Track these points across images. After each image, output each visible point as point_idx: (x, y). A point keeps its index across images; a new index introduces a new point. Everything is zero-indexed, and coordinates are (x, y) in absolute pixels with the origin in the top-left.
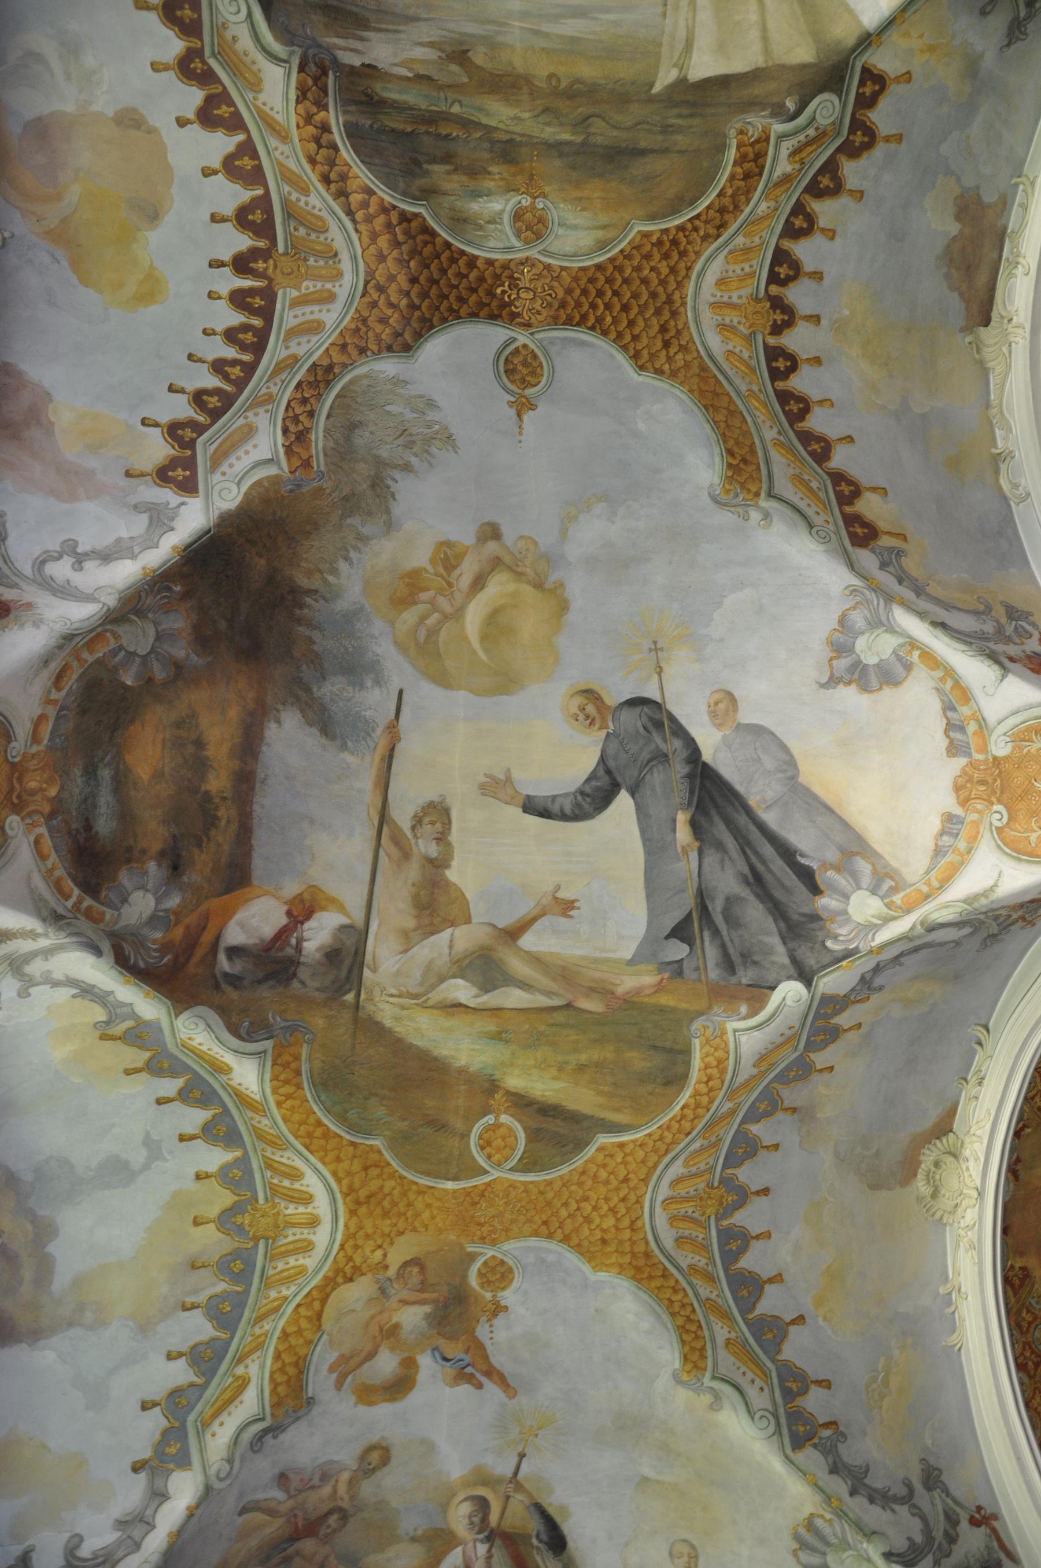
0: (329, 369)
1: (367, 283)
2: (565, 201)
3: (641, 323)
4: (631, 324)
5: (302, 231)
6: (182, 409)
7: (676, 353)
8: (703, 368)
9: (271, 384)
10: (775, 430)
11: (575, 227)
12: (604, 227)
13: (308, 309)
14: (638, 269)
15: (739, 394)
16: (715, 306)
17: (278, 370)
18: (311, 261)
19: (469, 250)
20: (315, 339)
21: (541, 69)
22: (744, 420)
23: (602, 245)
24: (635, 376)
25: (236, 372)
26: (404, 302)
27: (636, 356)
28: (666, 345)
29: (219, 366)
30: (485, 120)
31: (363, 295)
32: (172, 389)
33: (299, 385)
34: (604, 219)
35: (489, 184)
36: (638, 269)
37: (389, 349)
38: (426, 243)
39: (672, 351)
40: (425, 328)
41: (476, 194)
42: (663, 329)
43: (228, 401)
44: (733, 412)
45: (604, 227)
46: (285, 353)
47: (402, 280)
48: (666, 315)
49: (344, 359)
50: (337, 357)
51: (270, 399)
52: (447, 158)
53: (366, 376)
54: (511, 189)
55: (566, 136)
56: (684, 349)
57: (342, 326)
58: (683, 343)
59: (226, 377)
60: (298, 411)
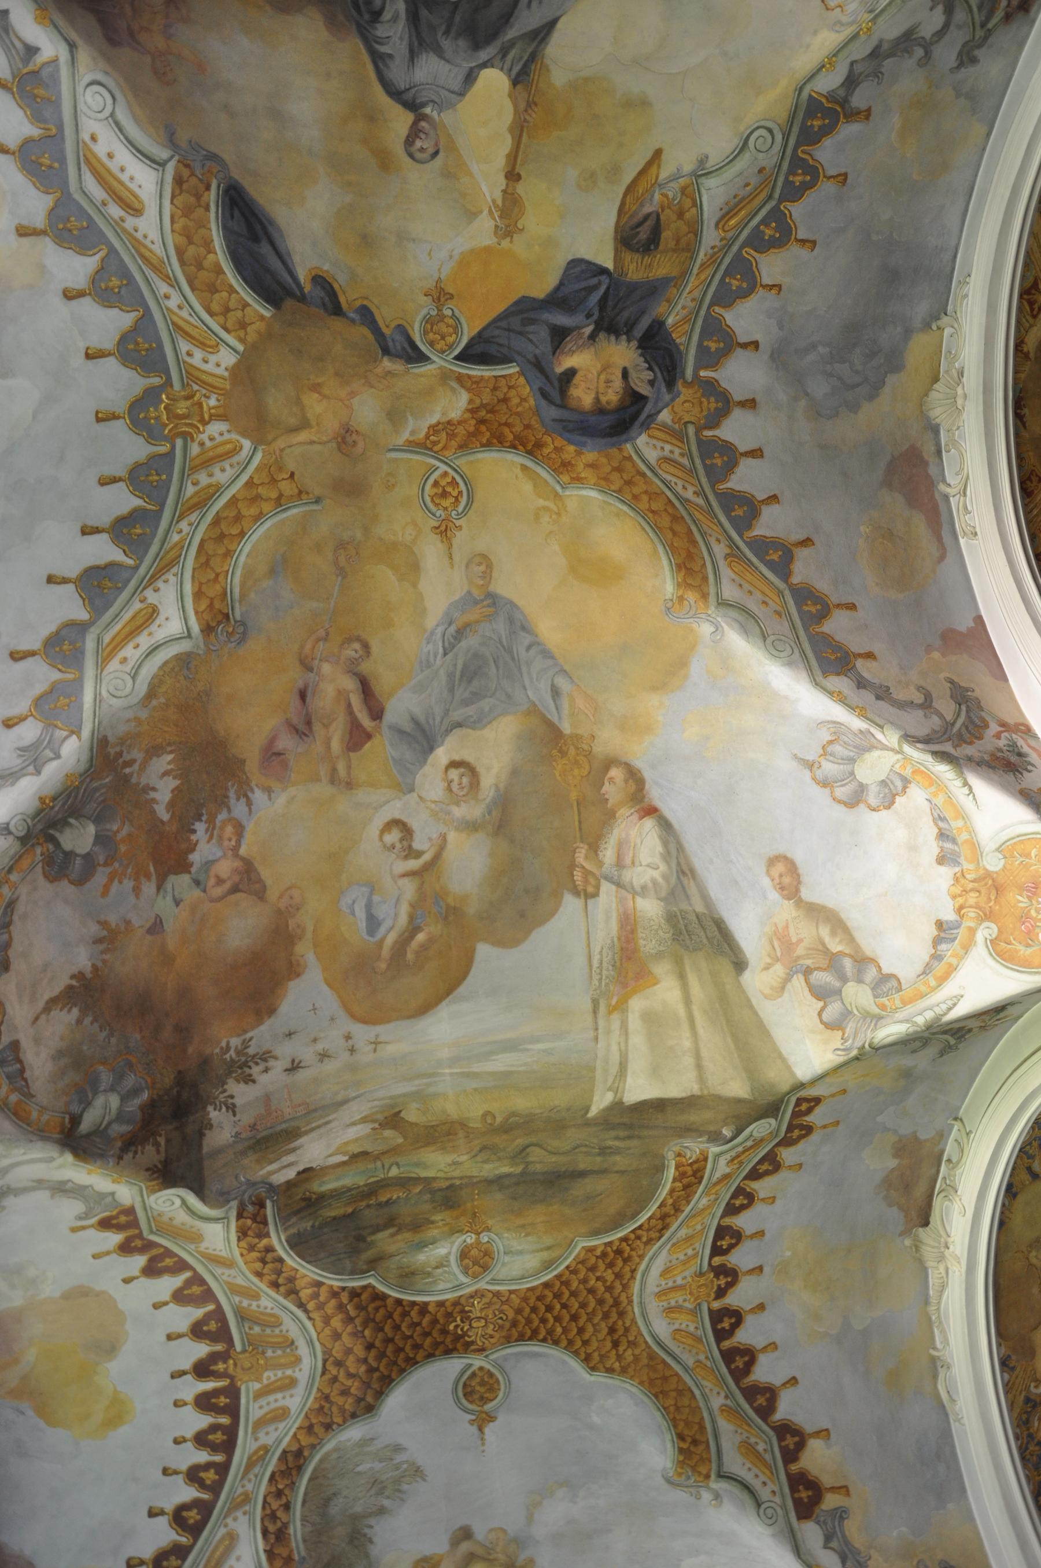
0: (299, 1453)
1: (325, 1361)
2: (508, 1230)
3: (590, 1329)
4: (581, 1331)
5: (257, 1329)
7: (625, 1350)
8: (652, 1356)
9: (245, 1482)
10: (723, 1394)
11: (520, 1253)
12: (549, 1248)
14: (584, 1281)
15: (686, 1369)
16: (661, 1294)
17: (250, 1465)
18: (269, 1353)
20: (281, 1426)
21: (474, 1110)
22: (693, 1396)
23: (548, 1265)
26: (363, 1369)
28: (616, 1344)
29: (193, 1475)
30: (424, 1174)
31: (323, 1373)
35: (434, 1232)
36: (584, 1281)
37: (354, 1416)
38: (377, 1309)
39: (621, 1349)
41: (422, 1246)
42: (612, 1330)
44: (683, 1391)
45: (549, 1248)
47: (359, 1350)
48: (614, 1316)
49: (312, 1440)
50: (305, 1441)
51: (247, 1498)
52: (390, 1222)
53: (336, 1449)
55: (505, 1170)
56: (632, 1344)
57: (306, 1409)
58: (631, 1338)
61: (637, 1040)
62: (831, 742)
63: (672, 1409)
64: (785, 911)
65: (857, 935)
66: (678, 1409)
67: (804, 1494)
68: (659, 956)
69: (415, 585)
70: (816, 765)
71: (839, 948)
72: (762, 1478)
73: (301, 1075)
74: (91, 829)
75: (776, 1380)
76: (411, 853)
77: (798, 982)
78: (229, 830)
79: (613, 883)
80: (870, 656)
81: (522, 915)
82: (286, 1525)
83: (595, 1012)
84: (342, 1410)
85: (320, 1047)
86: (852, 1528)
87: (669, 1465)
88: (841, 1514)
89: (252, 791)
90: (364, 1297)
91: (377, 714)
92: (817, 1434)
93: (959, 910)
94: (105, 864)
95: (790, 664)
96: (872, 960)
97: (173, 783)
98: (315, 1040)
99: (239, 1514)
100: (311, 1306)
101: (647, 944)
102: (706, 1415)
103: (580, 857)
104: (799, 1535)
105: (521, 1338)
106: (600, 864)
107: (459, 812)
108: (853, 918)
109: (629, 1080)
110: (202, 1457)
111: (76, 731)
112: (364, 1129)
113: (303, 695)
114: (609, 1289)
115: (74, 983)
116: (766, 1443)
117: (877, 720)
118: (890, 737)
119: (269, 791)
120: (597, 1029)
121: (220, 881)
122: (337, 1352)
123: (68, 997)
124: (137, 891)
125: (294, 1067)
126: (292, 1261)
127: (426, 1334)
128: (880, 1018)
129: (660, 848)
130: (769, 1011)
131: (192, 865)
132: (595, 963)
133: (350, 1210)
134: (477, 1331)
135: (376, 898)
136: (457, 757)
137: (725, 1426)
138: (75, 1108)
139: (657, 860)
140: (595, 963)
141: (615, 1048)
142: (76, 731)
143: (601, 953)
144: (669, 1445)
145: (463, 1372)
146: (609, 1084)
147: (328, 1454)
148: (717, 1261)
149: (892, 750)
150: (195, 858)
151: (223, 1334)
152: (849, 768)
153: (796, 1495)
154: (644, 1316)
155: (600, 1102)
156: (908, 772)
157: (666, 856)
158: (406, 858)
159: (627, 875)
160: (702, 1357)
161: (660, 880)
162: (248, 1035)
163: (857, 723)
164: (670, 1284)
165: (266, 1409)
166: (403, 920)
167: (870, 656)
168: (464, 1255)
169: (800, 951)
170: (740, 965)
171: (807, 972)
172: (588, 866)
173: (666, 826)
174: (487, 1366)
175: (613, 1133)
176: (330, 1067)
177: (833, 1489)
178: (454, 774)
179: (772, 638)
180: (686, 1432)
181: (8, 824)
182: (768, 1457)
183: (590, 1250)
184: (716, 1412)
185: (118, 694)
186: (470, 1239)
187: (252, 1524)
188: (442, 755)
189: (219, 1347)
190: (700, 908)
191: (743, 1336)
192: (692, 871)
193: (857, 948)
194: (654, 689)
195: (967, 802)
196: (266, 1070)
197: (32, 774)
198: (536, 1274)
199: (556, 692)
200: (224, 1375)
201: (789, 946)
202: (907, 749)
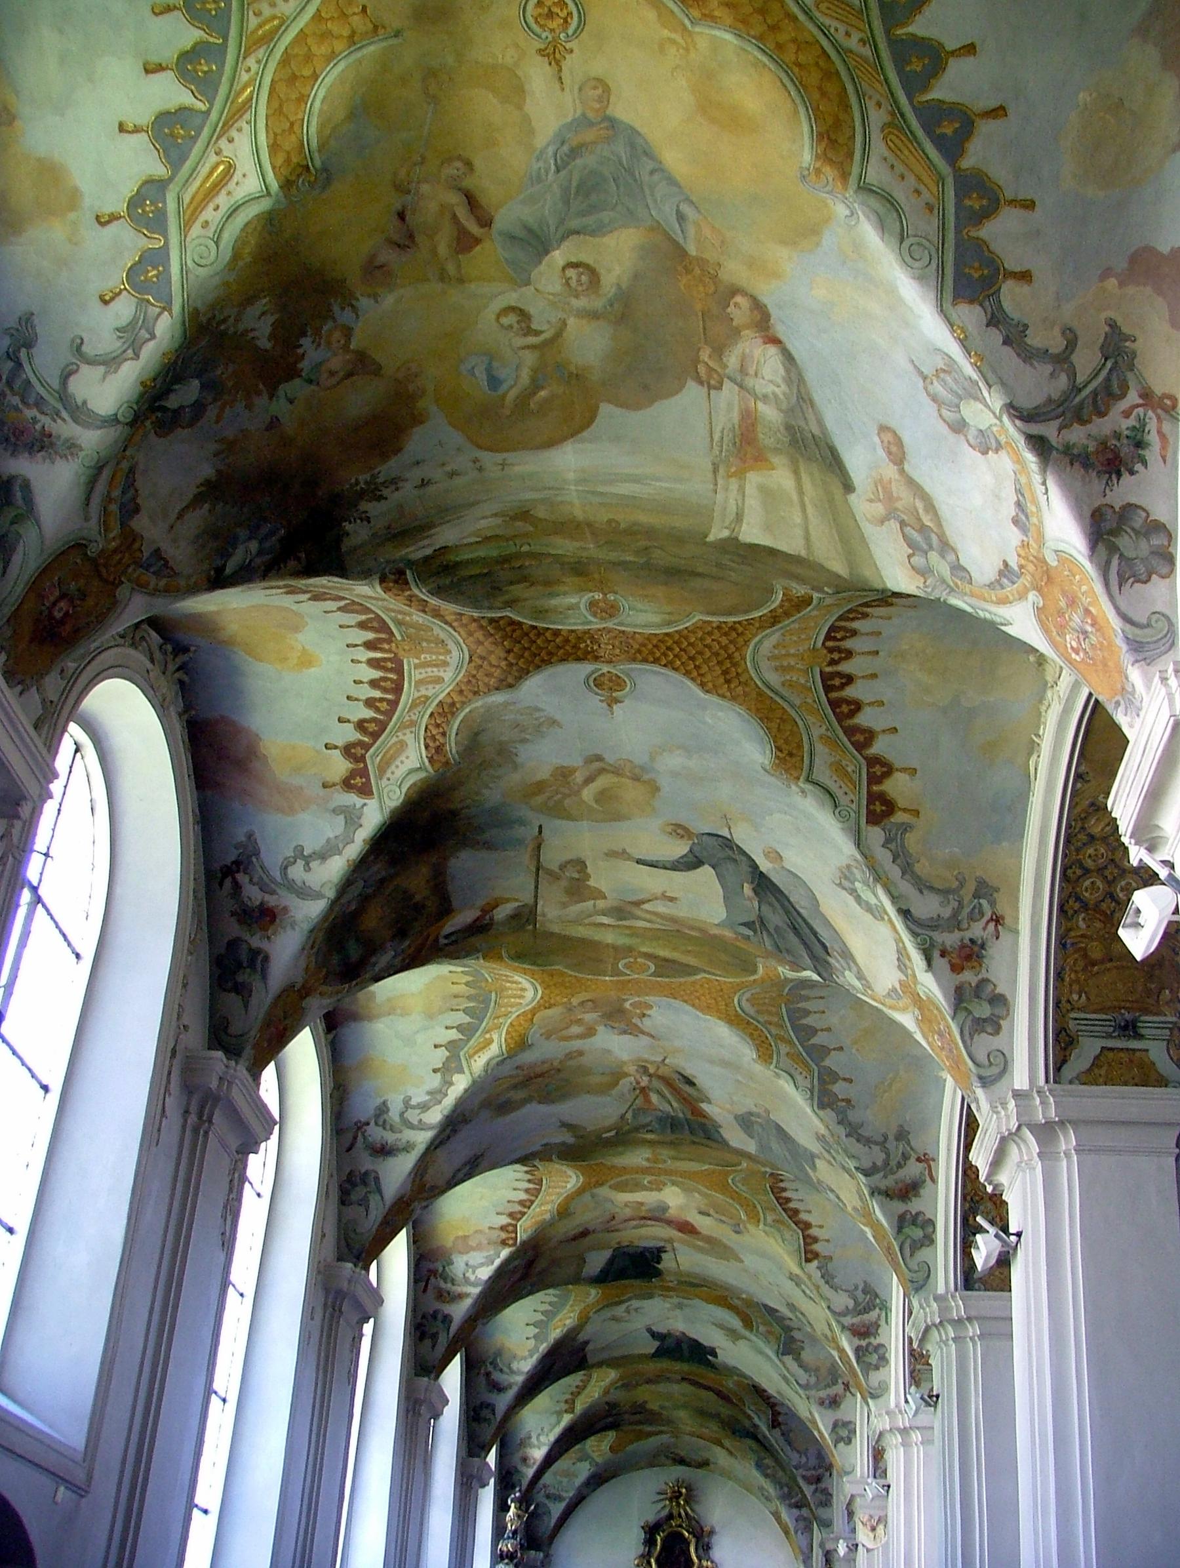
0: (453, 704)
4: (697, 667)
5: (412, 631)
6: (350, 734)
8: (761, 694)
13: (429, 669)
14: (701, 639)
15: (793, 706)
19: (551, 626)
20: (437, 687)
24: (702, 695)
25: (384, 706)
26: (503, 664)
27: (702, 685)
29: (370, 703)
30: (553, 552)
31: (471, 660)
32: (340, 720)
33: (432, 714)
34: (669, 609)
35: (562, 588)
37: (497, 689)
38: (514, 631)
39: (732, 686)
40: (524, 674)
41: (552, 595)
42: (725, 672)
43: (383, 726)
44: (785, 719)
46: (417, 695)
50: (457, 698)
51: (413, 724)
52: (524, 579)
54: (582, 590)
55: (631, 558)
56: (746, 684)
59: (377, 710)
60: (434, 732)
61: (753, 503)
62: (944, 371)
63: (775, 730)
64: (890, 471)
65: (944, 524)
66: (779, 730)
67: (879, 808)
68: (777, 451)
69: (520, 107)
70: (928, 381)
71: (928, 524)
72: (845, 789)
73: (431, 489)
74: (196, 383)
75: (877, 726)
76: (529, 332)
77: (894, 525)
78: (337, 335)
79: (736, 383)
80: (1025, 276)
81: (646, 387)
82: (443, 745)
83: (715, 471)
84: (487, 685)
85: (448, 468)
86: (912, 841)
87: (767, 762)
88: (906, 828)
89: (358, 300)
90: (501, 622)
91: (486, 222)
92: (903, 770)
93: (1021, 567)
94: (215, 400)
95: (920, 278)
96: (954, 550)
97: (270, 319)
98: (443, 465)
99: (407, 731)
100: (455, 624)
101: (766, 439)
102: (805, 739)
103: (705, 355)
104: (864, 833)
105: (645, 660)
106: (725, 366)
107: (577, 303)
108: (944, 511)
109: (744, 527)
110: (368, 714)
111: (167, 308)
112: (499, 521)
113: (401, 216)
114: (725, 648)
115: (203, 489)
116: (855, 764)
117: (990, 375)
118: (996, 400)
119: (375, 297)
120: (716, 485)
121: (332, 374)
122: (480, 650)
123: (197, 500)
124: (249, 407)
125: (424, 483)
126: (434, 601)
127: (559, 647)
128: (952, 590)
129: (782, 371)
130: (868, 529)
131: (302, 370)
132: (716, 437)
133: (485, 571)
134: (605, 650)
135: (495, 364)
136: (574, 260)
137: (820, 748)
138: (219, 563)
139: (779, 381)
140: (716, 437)
141: (732, 502)
142: (167, 308)
143: (722, 432)
144: (768, 752)
145: (593, 672)
146: (727, 524)
147: (476, 708)
148: (830, 644)
149: (994, 413)
150: (305, 365)
151: (383, 627)
152: (956, 401)
153: (872, 807)
154: (757, 669)
155: (718, 533)
156: (1003, 439)
157: (788, 381)
158: (525, 335)
159: (750, 382)
160: (810, 701)
161: (781, 396)
162: (376, 471)
163: (969, 371)
164: (783, 652)
165: (424, 675)
166: (525, 377)
167: (1025, 276)
168: (592, 604)
169: (899, 505)
170: (848, 487)
171: (903, 524)
172: (711, 364)
173: (788, 358)
174: (615, 672)
175: (727, 556)
176: (458, 481)
177: (905, 810)
178: (572, 273)
179: (912, 240)
180: (784, 746)
181: (116, 415)
182: (855, 777)
183: (705, 622)
184: (815, 738)
185: (203, 262)
186: (598, 596)
187: (417, 738)
188: (558, 257)
189: (383, 636)
190: (816, 431)
191: (850, 692)
192: (812, 403)
193: (944, 533)
194: (783, 242)
195: (1042, 499)
196: (397, 489)
197: (132, 359)
198: (659, 626)
199: (681, 217)
200: (390, 651)
201: (890, 498)
202: (1005, 418)
